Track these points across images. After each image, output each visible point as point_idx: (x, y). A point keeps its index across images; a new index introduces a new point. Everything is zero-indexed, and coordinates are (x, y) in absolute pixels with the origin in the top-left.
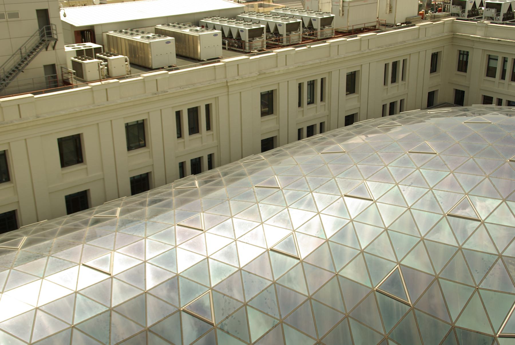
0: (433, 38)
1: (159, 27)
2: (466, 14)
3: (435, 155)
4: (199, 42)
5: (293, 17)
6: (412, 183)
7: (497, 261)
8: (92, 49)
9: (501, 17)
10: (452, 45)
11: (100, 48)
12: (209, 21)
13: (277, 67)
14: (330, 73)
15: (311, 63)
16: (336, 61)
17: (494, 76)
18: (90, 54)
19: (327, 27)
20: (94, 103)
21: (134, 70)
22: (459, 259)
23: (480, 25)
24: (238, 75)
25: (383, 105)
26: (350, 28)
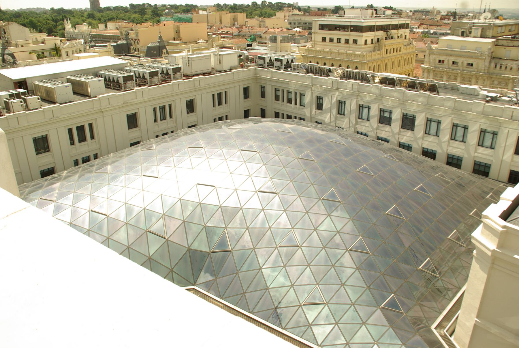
1: (69, 77)
2: (266, 64)
4: (88, 86)
5: (154, 68)
7: (218, 209)
8: (19, 93)
9: (283, 67)
11: (26, 92)
12: (103, 72)
13: (137, 98)
14: (174, 101)
15: (159, 95)
16: (177, 94)
17: (279, 100)
18: (18, 96)
20: (9, 126)
21: (44, 103)
22: (199, 209)
23: (269, 71)
24: (109, 104)
26: (193, 74)
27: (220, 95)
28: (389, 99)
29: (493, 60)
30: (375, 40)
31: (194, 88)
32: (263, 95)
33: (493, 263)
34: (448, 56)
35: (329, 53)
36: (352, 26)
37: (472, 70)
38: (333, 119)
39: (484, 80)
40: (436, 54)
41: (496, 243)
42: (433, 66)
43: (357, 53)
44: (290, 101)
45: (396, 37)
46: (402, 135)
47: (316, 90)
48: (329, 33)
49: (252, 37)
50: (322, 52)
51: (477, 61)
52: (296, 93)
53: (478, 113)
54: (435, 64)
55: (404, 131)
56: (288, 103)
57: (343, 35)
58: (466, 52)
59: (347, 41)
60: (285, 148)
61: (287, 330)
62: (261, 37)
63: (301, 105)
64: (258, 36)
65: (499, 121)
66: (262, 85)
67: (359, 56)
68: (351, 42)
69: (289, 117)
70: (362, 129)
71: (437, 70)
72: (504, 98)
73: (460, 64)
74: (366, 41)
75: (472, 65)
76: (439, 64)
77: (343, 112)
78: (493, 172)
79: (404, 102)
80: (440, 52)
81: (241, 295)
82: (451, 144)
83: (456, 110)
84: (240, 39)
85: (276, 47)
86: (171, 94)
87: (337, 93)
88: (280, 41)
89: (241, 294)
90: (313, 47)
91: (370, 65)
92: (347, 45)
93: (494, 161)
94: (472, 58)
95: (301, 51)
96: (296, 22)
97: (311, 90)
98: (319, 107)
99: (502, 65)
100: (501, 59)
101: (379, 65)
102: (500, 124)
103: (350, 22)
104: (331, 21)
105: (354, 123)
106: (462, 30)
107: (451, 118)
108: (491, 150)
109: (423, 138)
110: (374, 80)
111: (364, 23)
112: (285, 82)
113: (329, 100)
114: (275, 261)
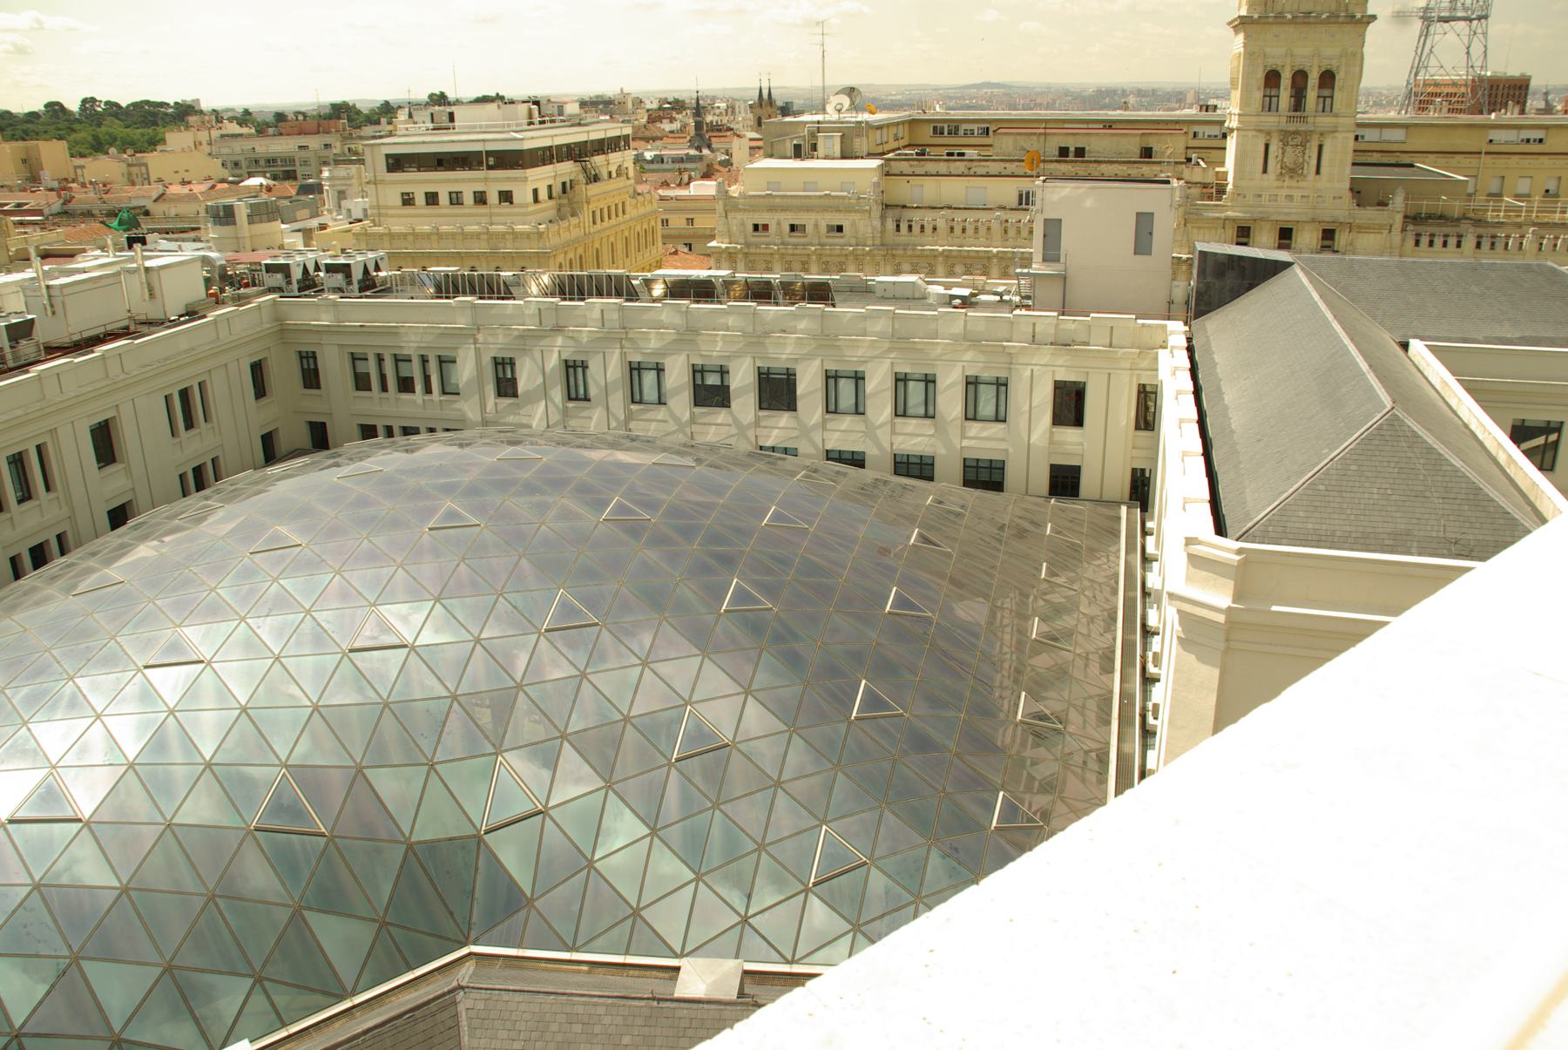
0: (244, 335)
2: (295, 286)
3: (300, 548)
6: (270, 610)
7: (450, 707)
9: (356, 286)
10: (283, 343)
14: (53, 432)
19: (23, 342)
22: (389, 725)
25: (181, 476)
26: (76, 338)
27: (185, 395)
28: (717, 335)
29: (890, 213)
30: (557, 190)
31: (109, 382)
32: (311, 377)
33: (1227, 640)
34: (776, 211)
35: (434, 238)
36: (489, 153)
37: (802, 240)
38: (555, 417)
39: (878, 264)
40: (745, 210)
41: (1230, 592)
42: (742, 241)
43: (519, 228)
44: (406, 385)
45: (606, 176)
46: (765, 427)
47: (491, 340)
48: (419, 182)
49: (125, 215)
50: (410, 238)
51: (851, 218)
52: (424, 360)
53: (955, 338)
54: (745, 237)
55: (769, 416)
56: (400, 391)
57: (467, 182)
58: (821, 197)
59: (480, 198)
60: (550, 499)
61: (805, 961)
62: (147, 213)
63: (444, 393)
64: (137, 211)
65: (1007, 351)
66: (304, 349)
67: (528, 235)
68: (493, 198)
69: (408, 431)
70: (648, 430)
71: (753, 250)
72: (983, 298)
73: (809, 229)
74: (535, 191)
75: (840, 229)
76: (756, 234)
77: (581, 391)
78: (1012, 477)
79: (759, 337)
80: (751, 203)
81: (629, 922)
82: (898, 429)
83: (899, 340)
84: (83, 226)
85: (237, 238)
86: (42, 409)
87: (560, 341)
88: (245, 219)
89: (625, 919)
90: (375, 226)
91: (560, 258)
92: (482, 210)
93: (1011, 450)
94: (838, 211)
95: (335, 242)
96: (241, 158)
97: (475, 343)
98: (506, 387)
99: (913, 223)
100: (904, 207)
101: (581, 256)
102: (1010, 357)
103: (484, 141)
104: (424, 142)
105: (623, 417)
106: (795, 142)
107: (889, 360)
108: (1001, 426)
109: (823, 425)
110: (650, 290)
111: (525, 142)
112: (385, 330)
113: (536, 363)
114: (686, 799)
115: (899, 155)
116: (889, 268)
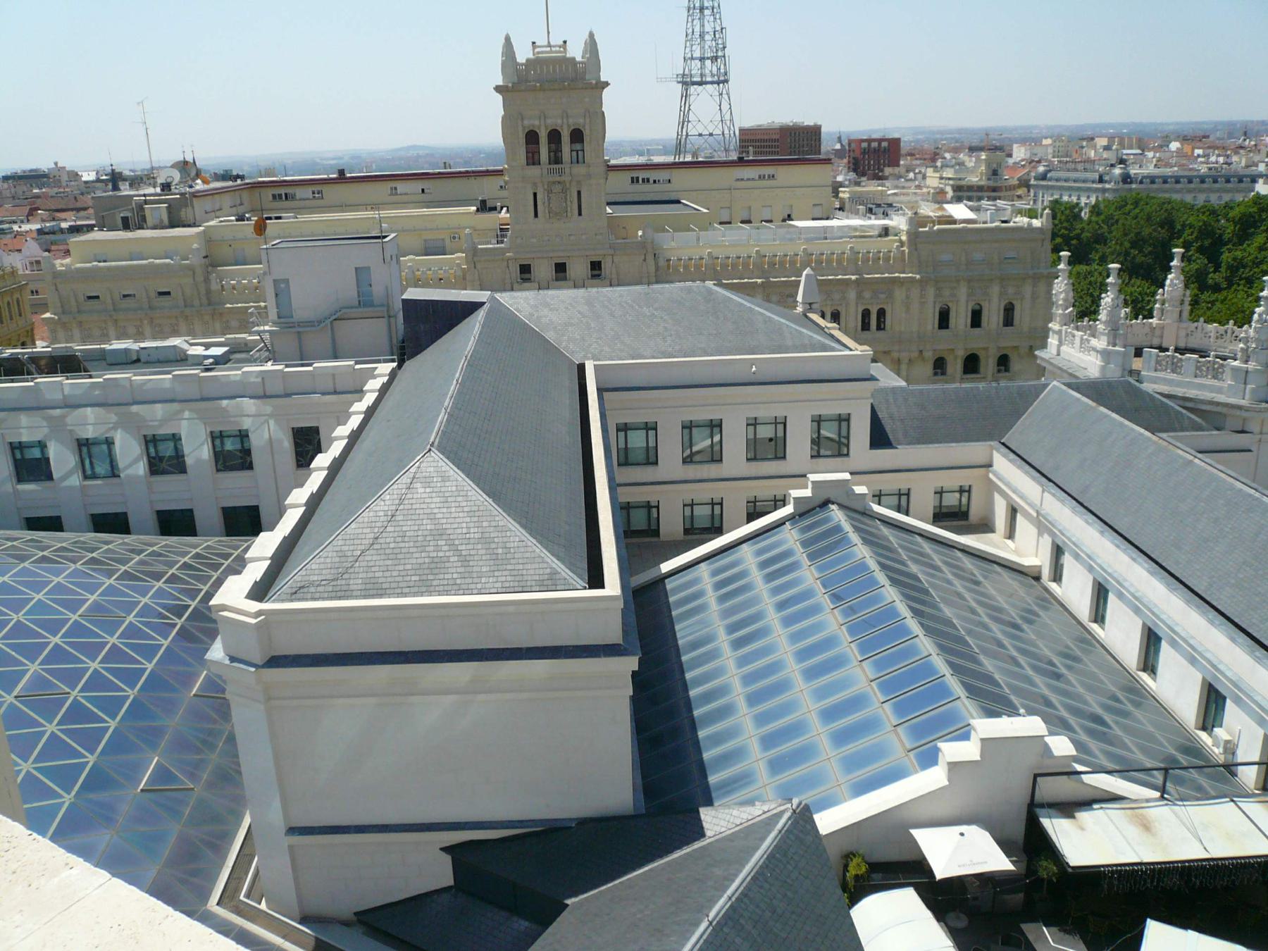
106: (122, 215)
115: (221, 221)
116: (218, 325)
